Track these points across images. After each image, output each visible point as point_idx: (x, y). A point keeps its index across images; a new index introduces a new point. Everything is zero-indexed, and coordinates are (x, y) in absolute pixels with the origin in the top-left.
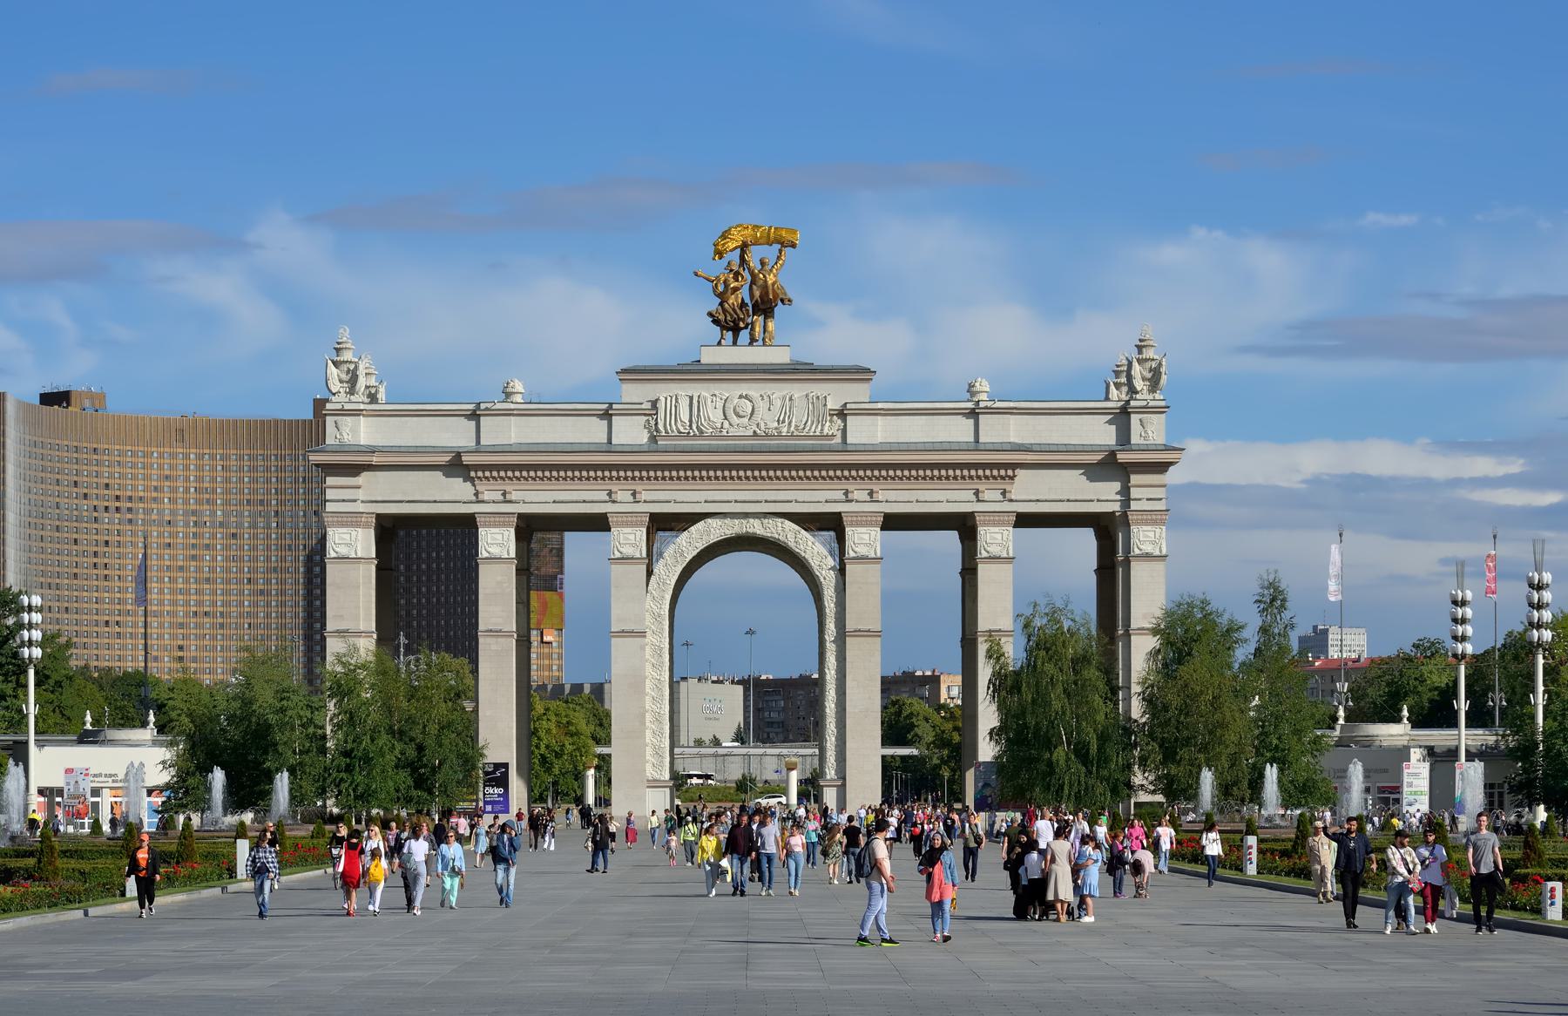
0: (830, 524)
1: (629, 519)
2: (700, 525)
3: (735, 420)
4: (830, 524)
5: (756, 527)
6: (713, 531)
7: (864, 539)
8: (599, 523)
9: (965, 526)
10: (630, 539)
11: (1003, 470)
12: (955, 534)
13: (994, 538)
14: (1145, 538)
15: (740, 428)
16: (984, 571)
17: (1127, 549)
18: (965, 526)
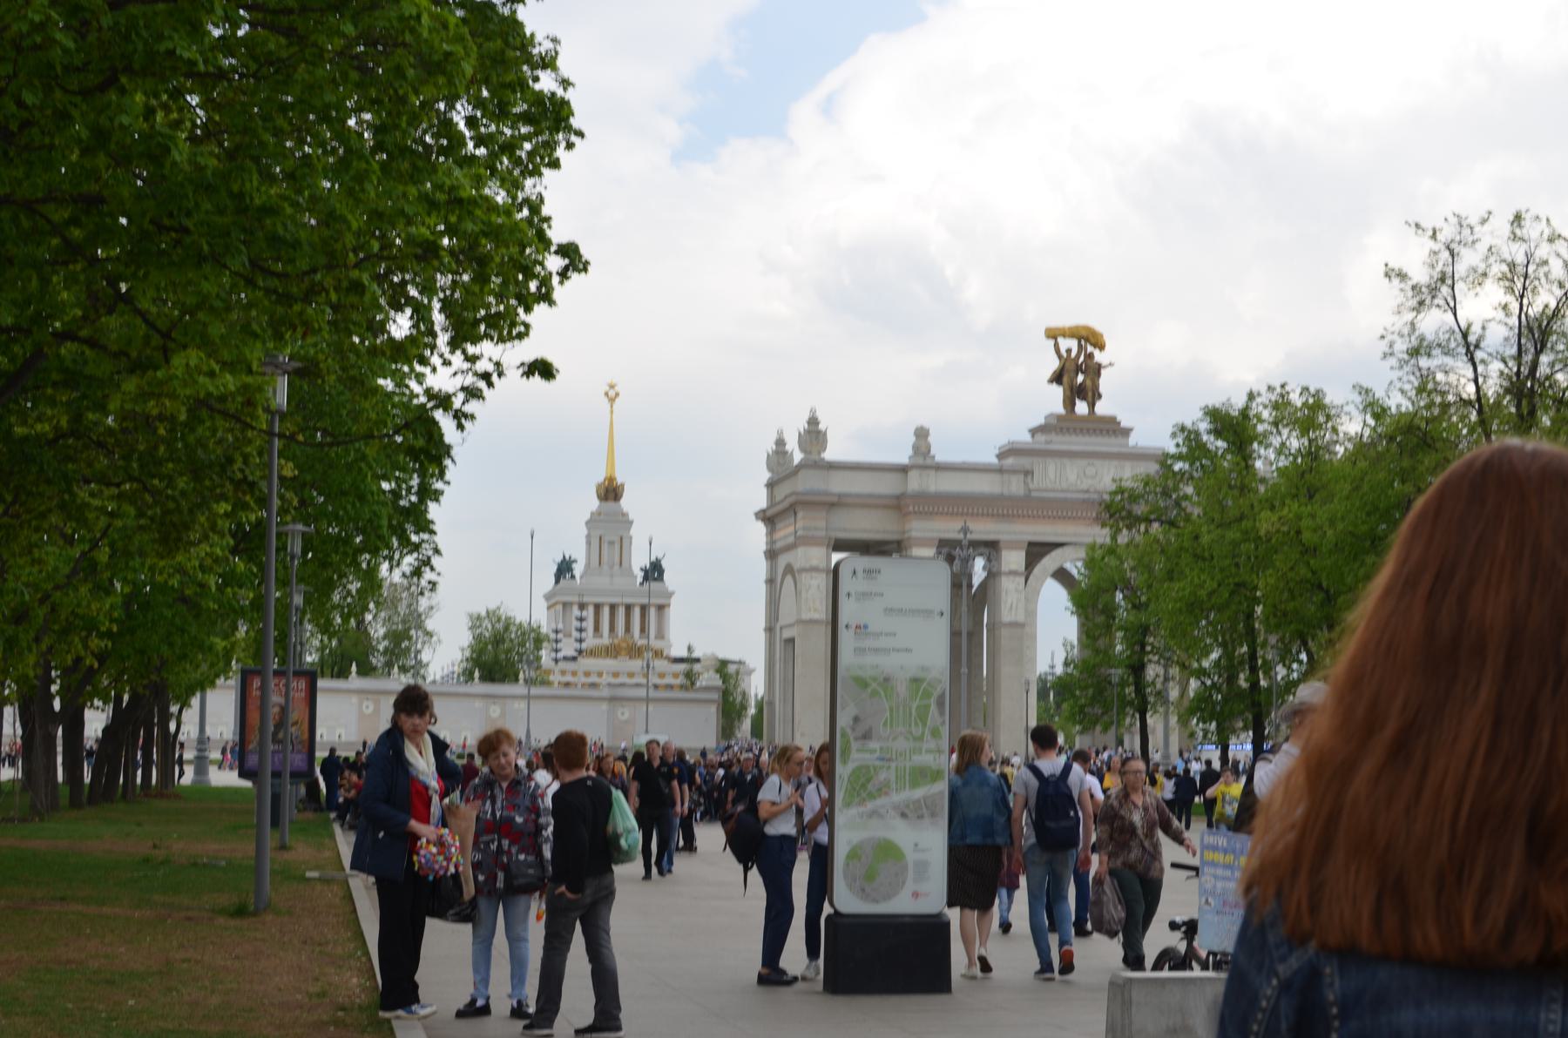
1: (1013, 545)
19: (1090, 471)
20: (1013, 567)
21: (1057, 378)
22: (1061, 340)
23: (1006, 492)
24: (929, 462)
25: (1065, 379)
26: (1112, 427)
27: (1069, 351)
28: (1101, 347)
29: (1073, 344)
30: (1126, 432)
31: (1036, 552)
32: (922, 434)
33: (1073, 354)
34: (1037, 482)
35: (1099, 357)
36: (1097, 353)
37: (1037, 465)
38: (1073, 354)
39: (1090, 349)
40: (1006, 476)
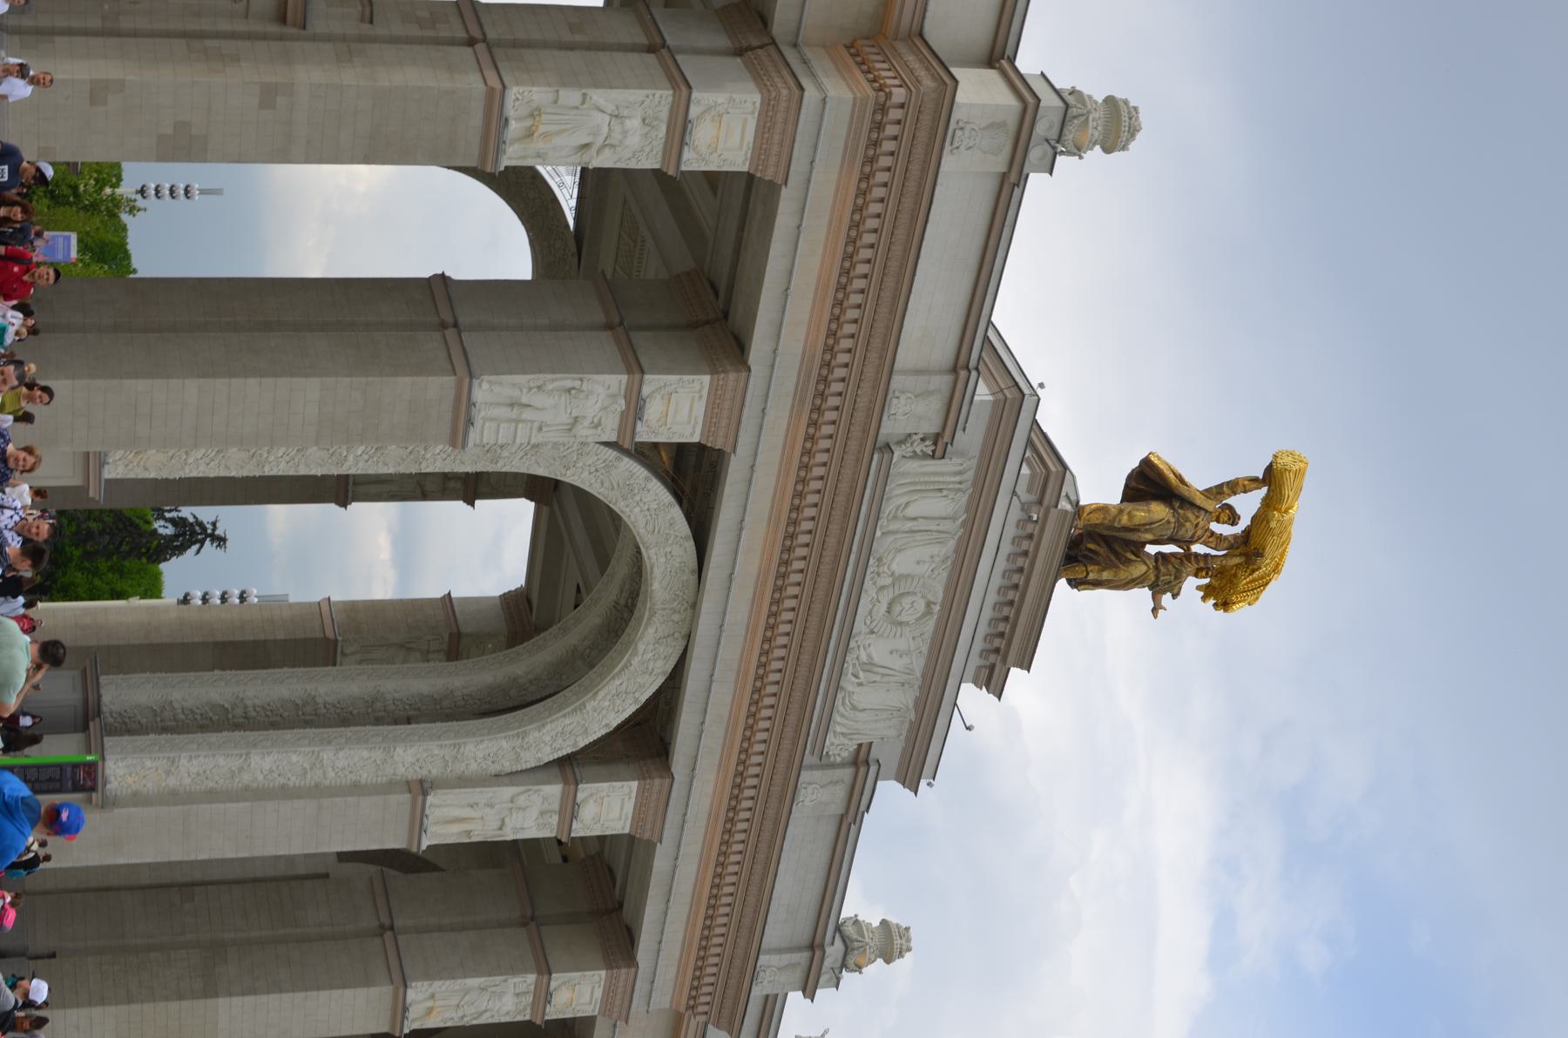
2: (683, 527)
3: (885, 599)
7: (608, 807)
10: (679, 406)
15: (873, 602)
19: (912, 608)
20: (653, 410)
22: (1265, 489)
23: (897, 381)
24: (1035, 153)
25: (1159, 511)
26: (1011, 645)
27: (1233, 519)
30: (993, 682)
31: (692, 475)
32: (1115, 126)
34: (907, 468)
35: (1191, 585)
37: (959, 466)
38: (1214, 526)
40: (942, 382)
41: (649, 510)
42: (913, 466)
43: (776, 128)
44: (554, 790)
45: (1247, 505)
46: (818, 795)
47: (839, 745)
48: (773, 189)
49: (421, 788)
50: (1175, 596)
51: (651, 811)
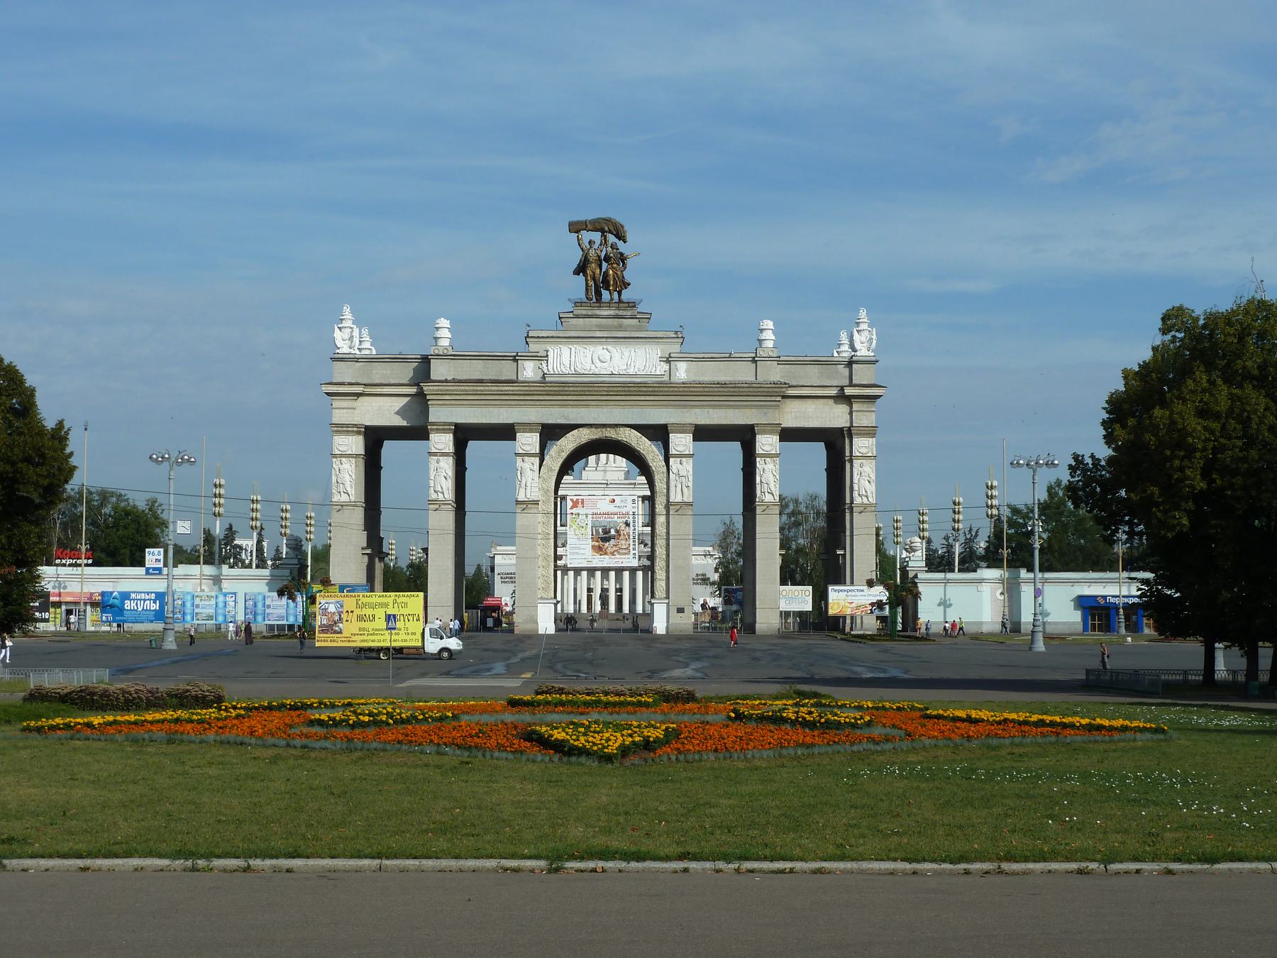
0: (659, 434)
1: (528, 427)
3: (599, 364)
4: (659, 434)
5: (611, 434)
6: (582, 436)
7: (681, 442)
8: (506, 432)
9: (746, 436)
10: (528, 441)
11: (780, 393)
12: (738, 444)
13: (767, 443)
14: (861, 445)
15: (604, 369)
16: (759, 462)
17: (851, 451)
18: (746, 436)
20: (528, 449)
21: (581, 269)
28: (621, 236)
29: (597, 236)
33: (596, 246)
36: (620, 244)
39: (612, 239)
41: (568, 443)
42: (550, 367)
43: (442, 428)
44: (672, 460)
45: (586, 236)
46: (682, 372)
47: (662, 368)
48: (457, 425)
49: (668, 505)
50: (622, 254)
51: (681, 429)
